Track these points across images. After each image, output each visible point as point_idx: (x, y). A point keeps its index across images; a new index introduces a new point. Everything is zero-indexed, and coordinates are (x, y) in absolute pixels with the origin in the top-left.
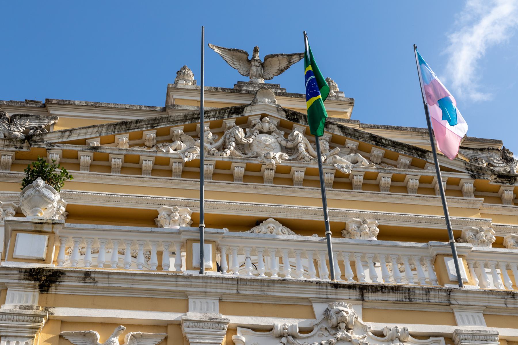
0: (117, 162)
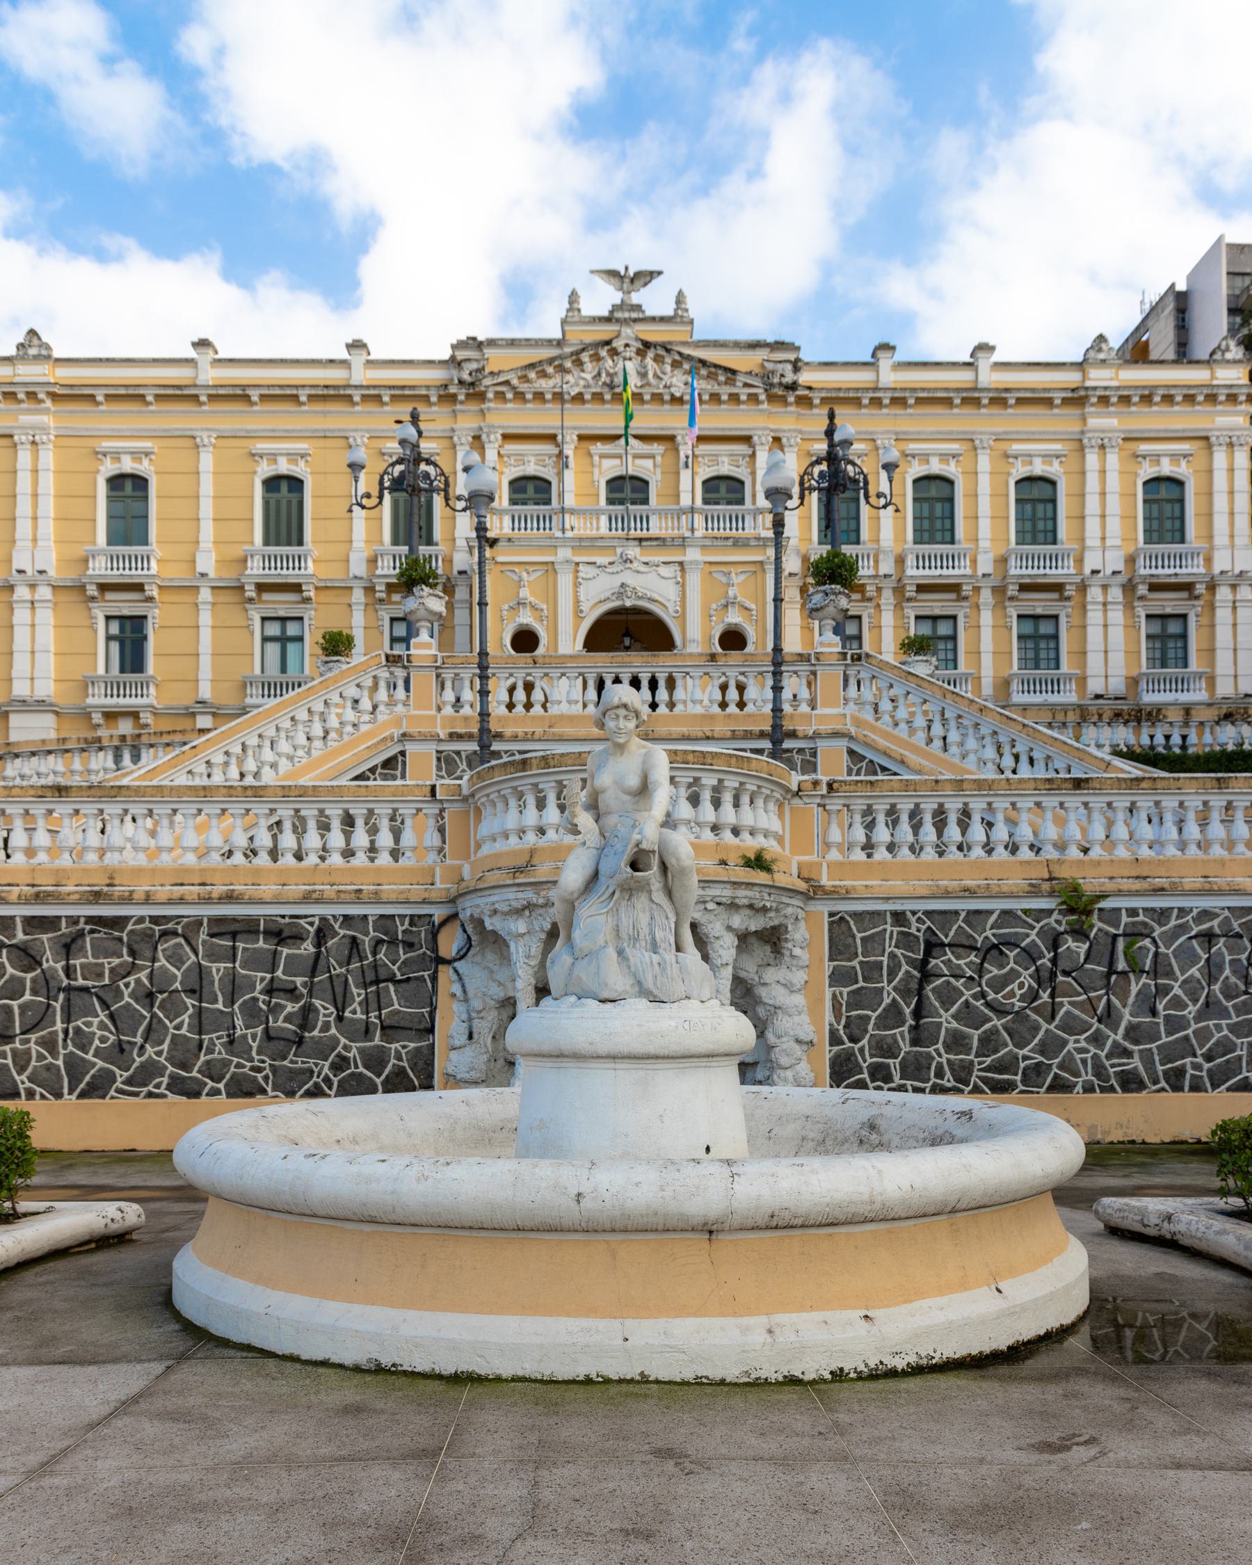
0: (529, 396)
